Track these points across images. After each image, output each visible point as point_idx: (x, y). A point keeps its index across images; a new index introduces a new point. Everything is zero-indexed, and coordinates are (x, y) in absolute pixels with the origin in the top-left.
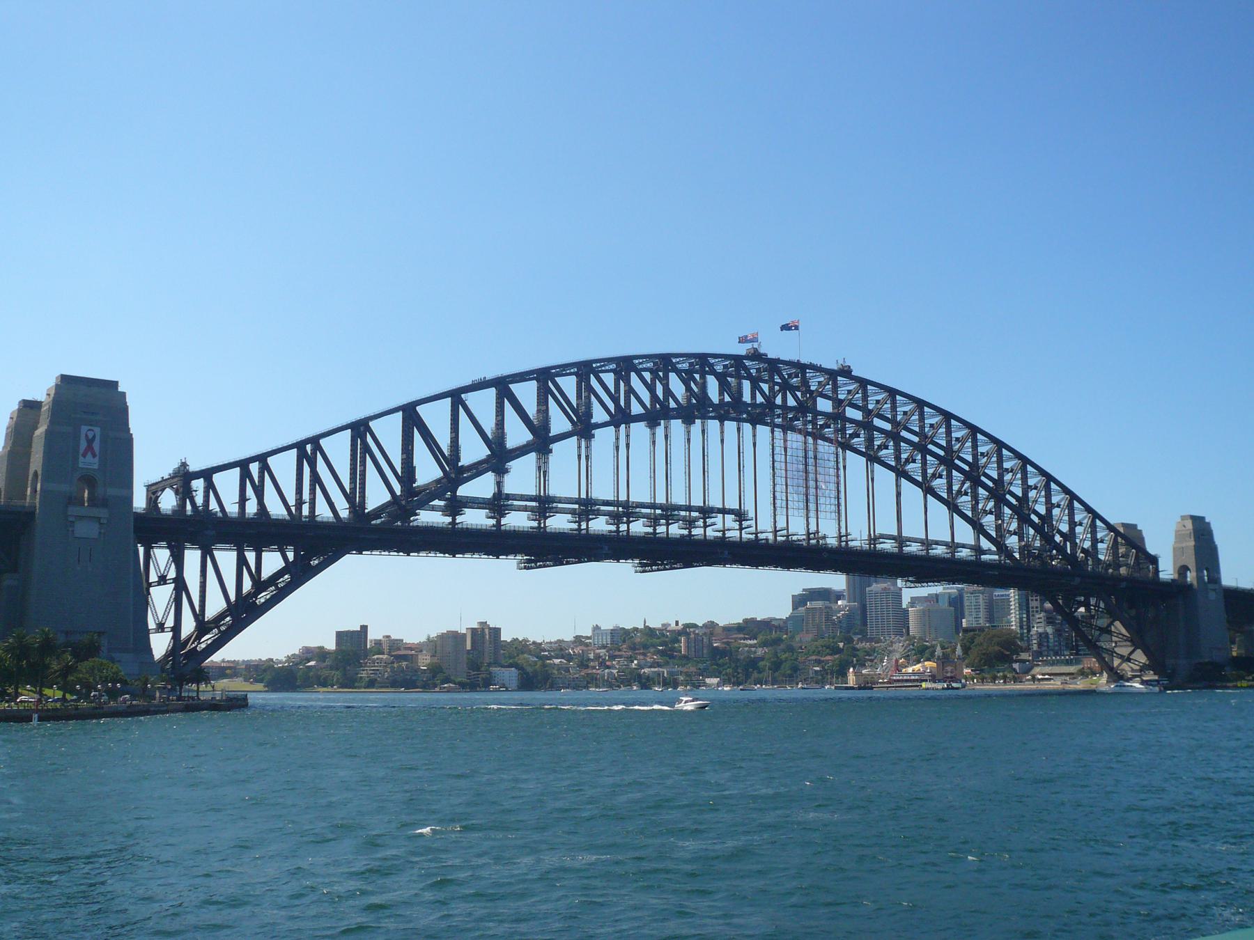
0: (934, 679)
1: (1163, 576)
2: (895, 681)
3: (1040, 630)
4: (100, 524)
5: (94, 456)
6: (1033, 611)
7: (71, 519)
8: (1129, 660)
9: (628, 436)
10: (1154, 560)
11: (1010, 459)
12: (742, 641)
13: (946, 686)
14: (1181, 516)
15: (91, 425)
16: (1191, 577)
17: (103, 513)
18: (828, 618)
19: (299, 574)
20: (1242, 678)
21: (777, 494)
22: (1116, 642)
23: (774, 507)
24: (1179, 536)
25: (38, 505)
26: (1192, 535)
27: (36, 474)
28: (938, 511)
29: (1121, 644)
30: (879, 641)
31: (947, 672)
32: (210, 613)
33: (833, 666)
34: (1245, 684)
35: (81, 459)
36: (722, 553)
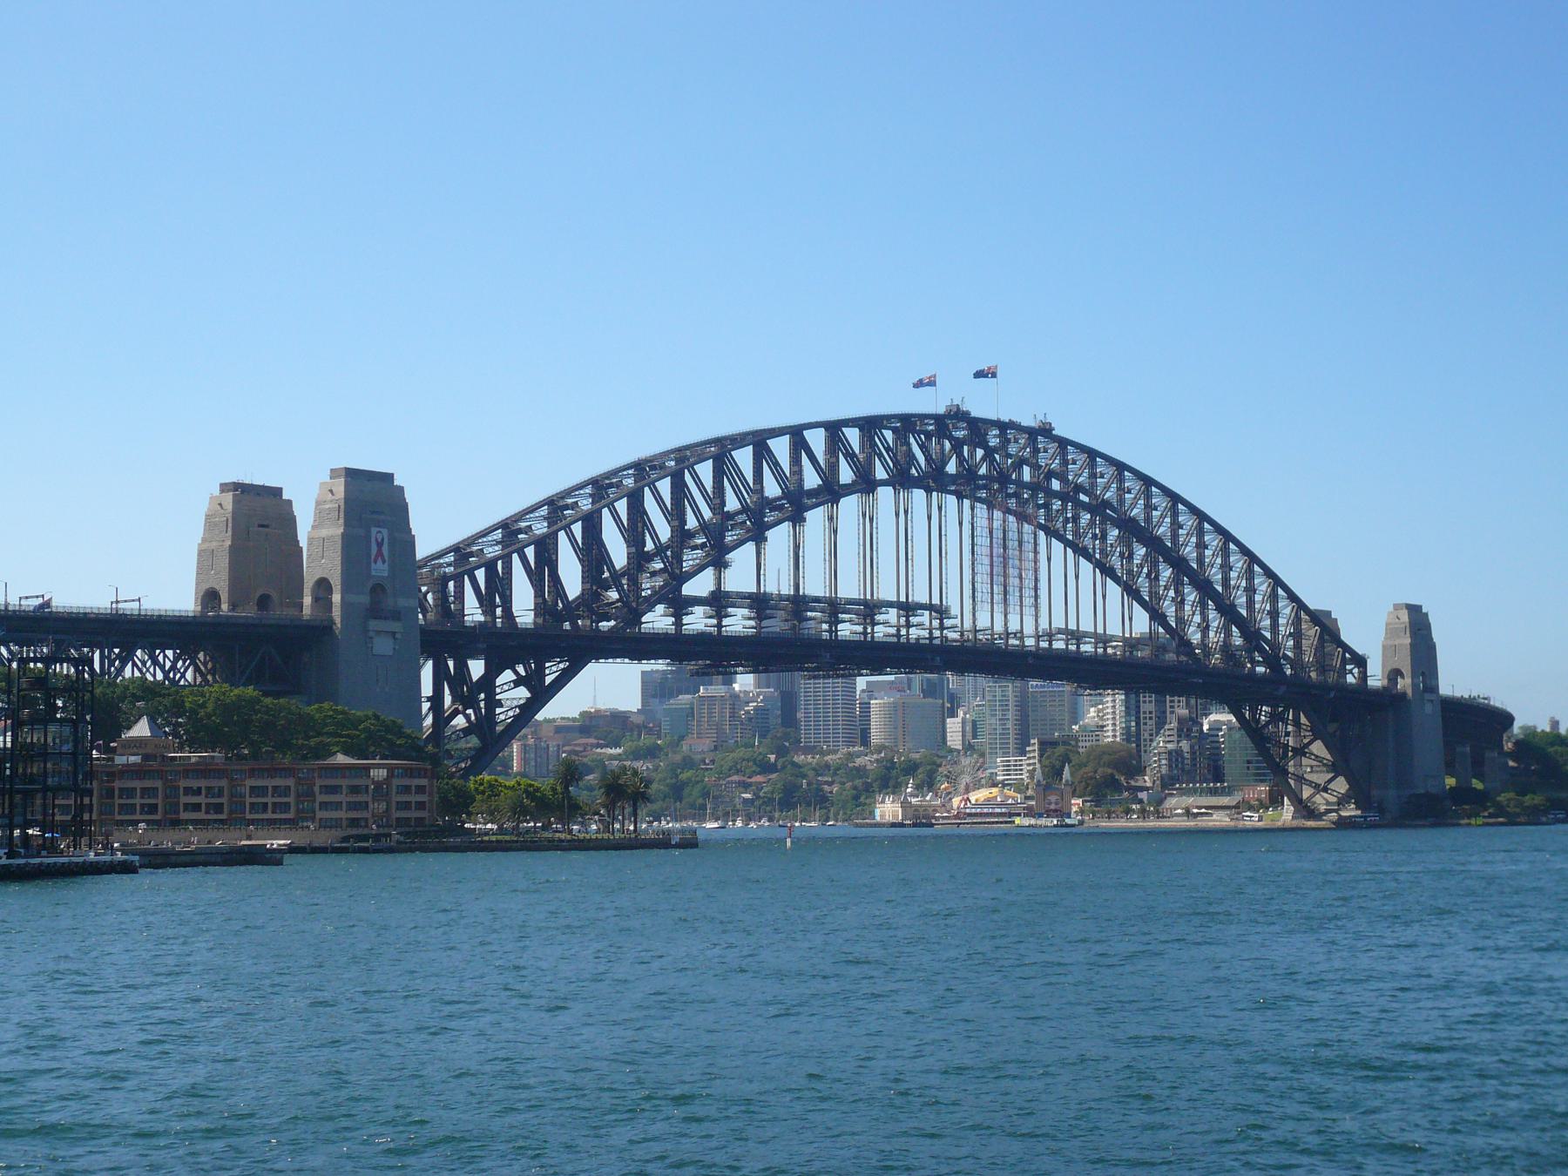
0: (1030, 812)
1: (1371, 683)
2: (970, 815)
3: (1170, 746)
5: (384, 562)
6: (1145, 718)
7: (371, 634)
8: (1325, 790)
10: (1361, 662)
12: (599, 750)
13: (1055, 822)
14: (1394, 605)
15: (379, 527)
16: (1404, 684)
17: (395, 626)
18: (733, 715)
20: (1477, 815)
21: (978, 586)
22: (1312, 767)
23: (974, 600)
24: (1391, 631)
25: (338, 620)
29: (1318, 769)
30: (823, 753)
31: (1050, 804)
33: (772, 793)
34: (1480, 821)
35: (373, 564)
36: (933, 659)
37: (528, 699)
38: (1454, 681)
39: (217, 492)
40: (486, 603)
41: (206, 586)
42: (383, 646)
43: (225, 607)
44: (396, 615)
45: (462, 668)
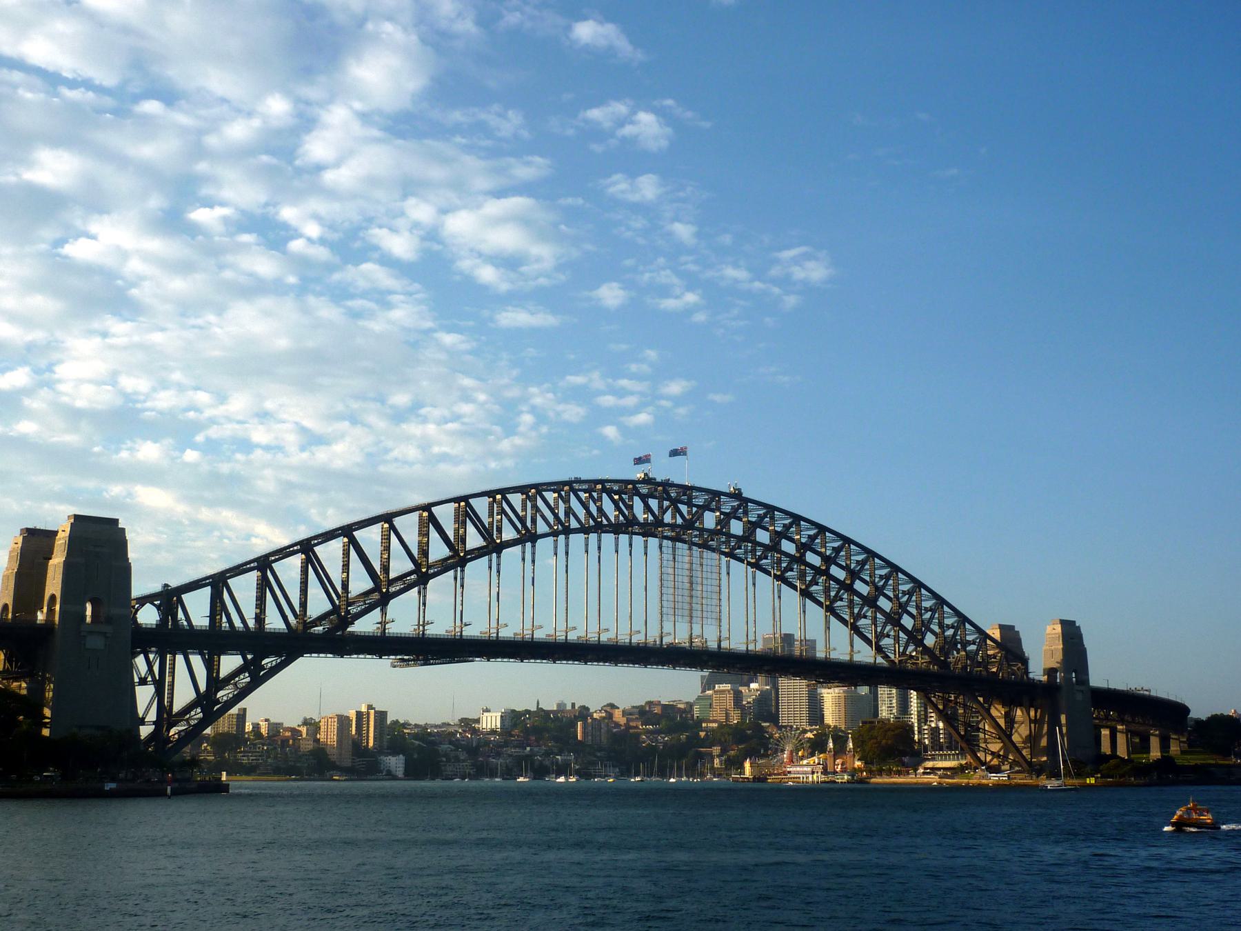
7: (82, 634)
9: (533, 554)
11: (882, 568)
19: (257, 676)
26: (1061, 638)
27: (53, 597)
28: (816, 613)
32: (177, 707)
38: (1102, 675)
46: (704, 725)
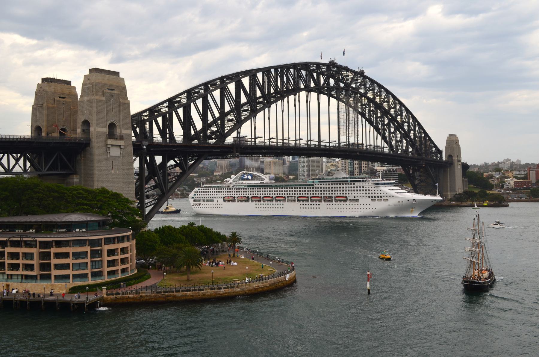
4: (121, 148)
7: (109, 146)
10: (440, 152)
37: (181, 173)
39: (40, 82)
40: (162, 133)
41: (35, 125)
42: (115, 152)
43: (43, 134)
44: (121, 138)
45: (153, 160)
46: (215, 174)
